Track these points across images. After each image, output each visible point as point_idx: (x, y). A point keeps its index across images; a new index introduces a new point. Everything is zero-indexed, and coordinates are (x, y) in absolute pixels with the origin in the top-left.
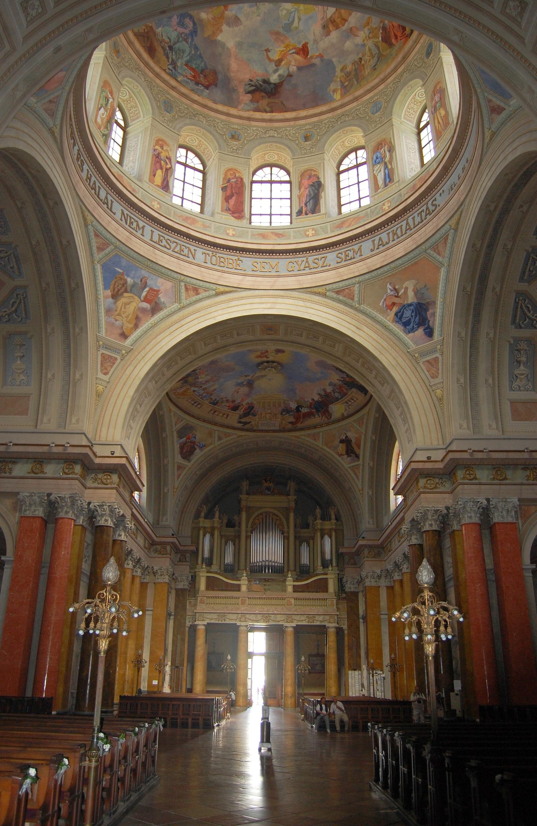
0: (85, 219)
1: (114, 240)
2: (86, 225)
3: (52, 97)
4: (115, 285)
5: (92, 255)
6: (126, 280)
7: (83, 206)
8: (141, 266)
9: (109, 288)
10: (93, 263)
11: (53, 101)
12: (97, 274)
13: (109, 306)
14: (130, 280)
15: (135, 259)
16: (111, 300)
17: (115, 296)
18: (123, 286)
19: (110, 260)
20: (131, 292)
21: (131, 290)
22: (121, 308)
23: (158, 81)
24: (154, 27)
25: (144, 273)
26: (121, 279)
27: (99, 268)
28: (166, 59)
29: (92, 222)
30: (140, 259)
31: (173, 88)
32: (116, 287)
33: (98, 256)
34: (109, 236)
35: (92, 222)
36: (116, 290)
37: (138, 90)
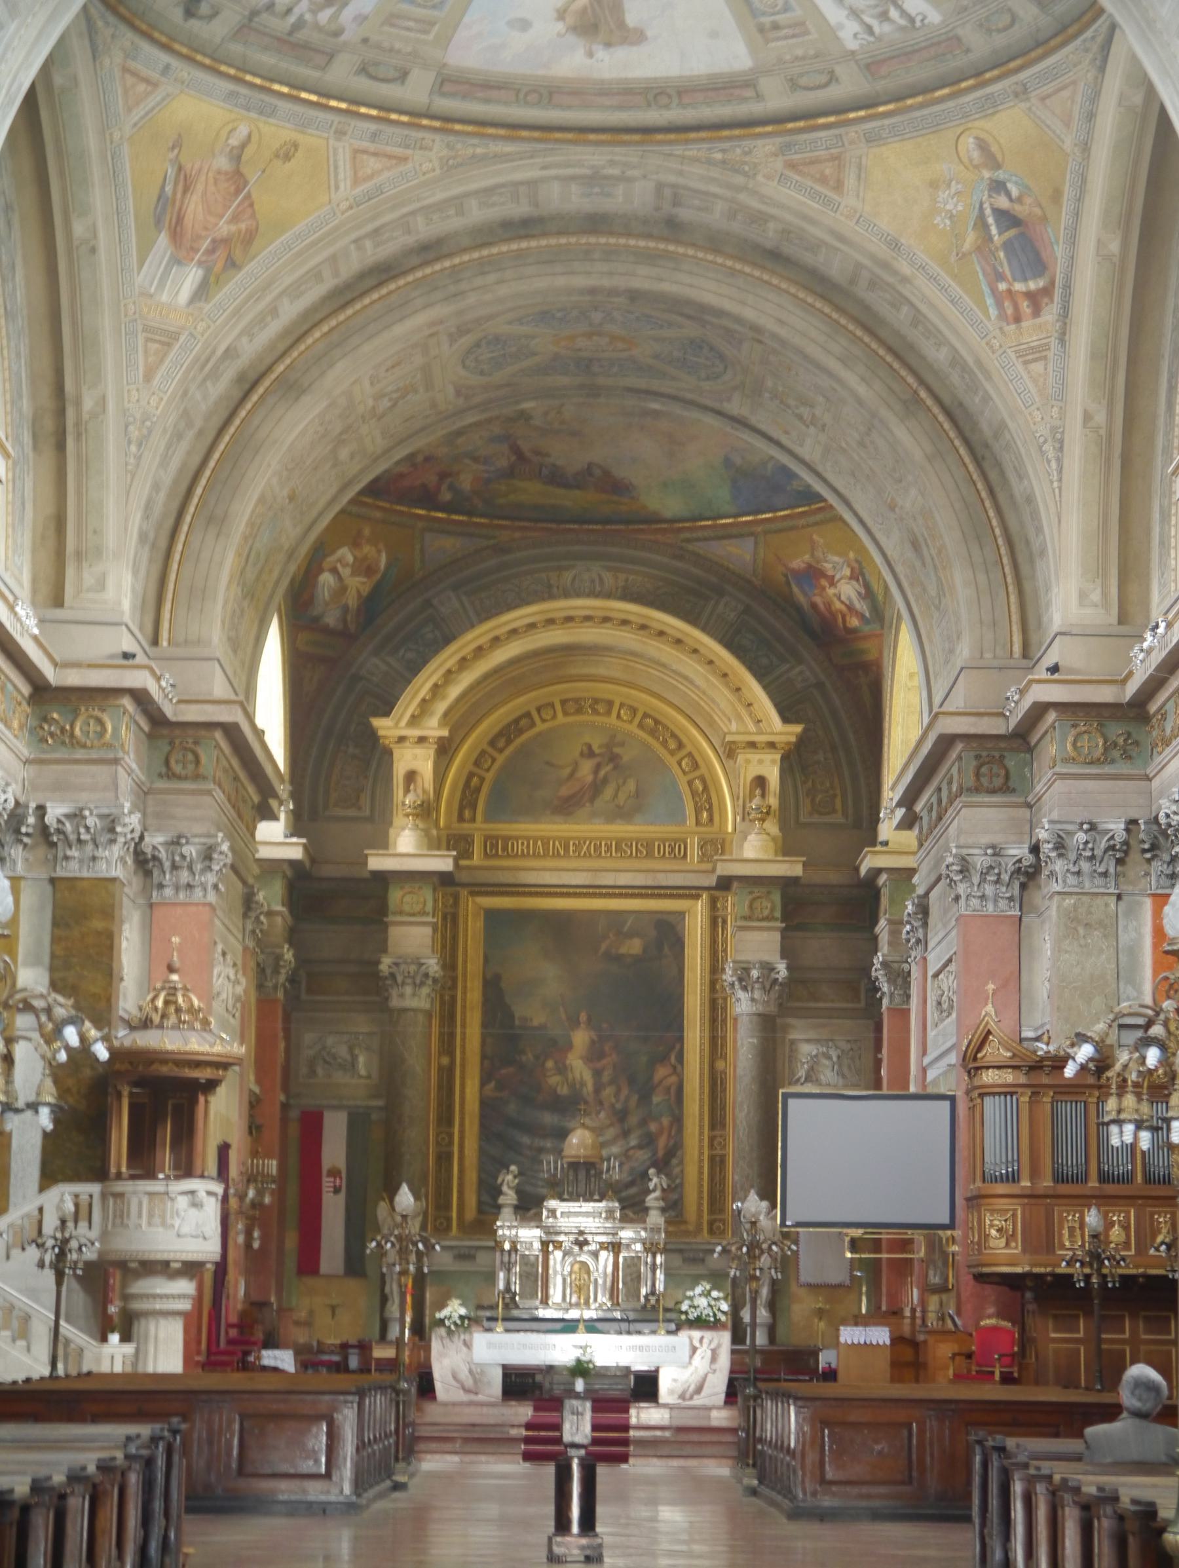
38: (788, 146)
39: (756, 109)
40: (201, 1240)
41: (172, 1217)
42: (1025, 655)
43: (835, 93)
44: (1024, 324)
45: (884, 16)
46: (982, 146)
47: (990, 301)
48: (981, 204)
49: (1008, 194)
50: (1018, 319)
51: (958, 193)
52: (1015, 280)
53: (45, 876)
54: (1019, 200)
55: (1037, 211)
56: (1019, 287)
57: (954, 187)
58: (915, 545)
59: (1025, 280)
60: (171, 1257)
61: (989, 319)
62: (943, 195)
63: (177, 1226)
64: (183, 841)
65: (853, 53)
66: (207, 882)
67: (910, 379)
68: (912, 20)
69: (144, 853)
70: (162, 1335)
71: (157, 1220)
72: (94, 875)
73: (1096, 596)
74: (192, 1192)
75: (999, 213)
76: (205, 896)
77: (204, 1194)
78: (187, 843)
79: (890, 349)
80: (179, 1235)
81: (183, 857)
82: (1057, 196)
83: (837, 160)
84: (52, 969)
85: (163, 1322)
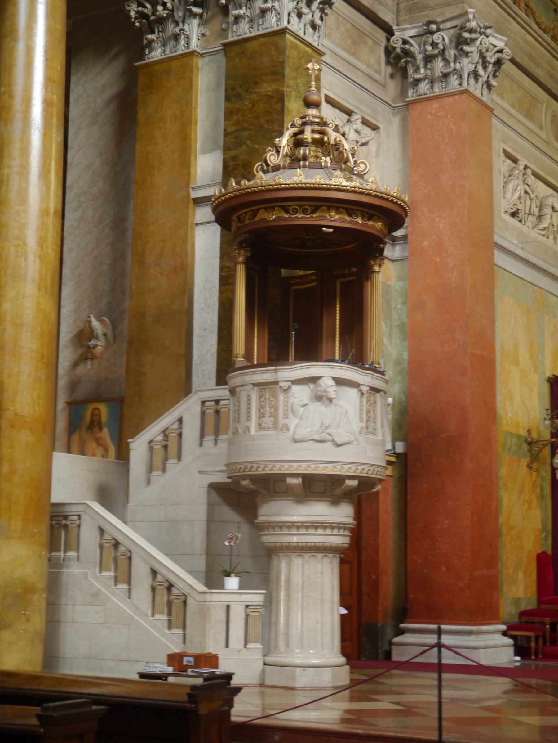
40: (329, 445)
41: (286, 416)
53: (217, 45)
60: (285, 469)
63: (292, 429)
64: (434, 27)
66: (462, 69)
69: (394, 48)
70: (297, 578)
71: (268, 420)
72: (262, 32)
74: (314, 380)
76: (460, 84)
77: (332, 383)
78: (439, 30)
80: (295, 441)
81: (434, 45)
84: (226, 149)
85: (297, 561)
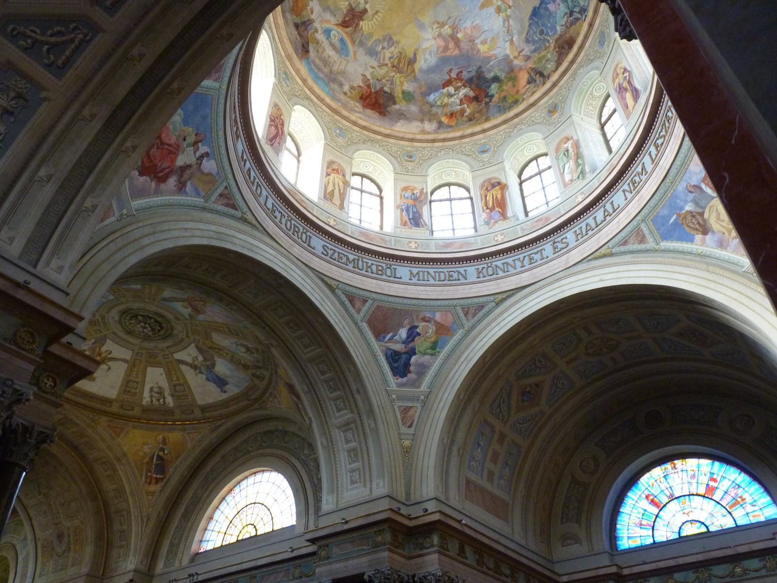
0: (605, 256)
1: (635, 223)
2: (611, 255)
3: (462, 315)
4: (690, 227)
5: (647, 251)
6: (687, 211)
7: (589, 258)
8: (672, 191)
9: (694, 235)
10: (657, 250)
11: (467, 311)
12: (672, 248)
13: (715, 241)
14: (689, 207)
15: (662, 197)
16: (709, 237)
17: (705, 230)
18: (694, 216)
19: (658, 229)
20: (704, 208)
21: (702, 207)
22: (723, 226)
23: (587, 45)
24: (556, 36)
25: (681, 187)
26: (685, 218)
27: (665, 245)
28: (579, 22)
29: (609, 248)
30: (661, 191)
31: (591, 25)
32: (693, 226)
33: (651, 244)
34: (629, 229)
35: (609, 248)
36: (697, 226)
37: (588, 80)
38: (111, 421)
39: (108, 409)
42: (102, 575)
43: (130, 413)
44: (151, 486)
45: (159, 400)
46: (164, 439)
47: (144, 477)
48: (154, 453)
49: (164, 452)
50: (150, 483)
51: (150, 448)
52: (154, 473)
54: (166, 455)
55: (170, 459)
56: (155, 476)
57: (150, 446)
58: (60, 537)
59: (157, 474)
61: (141, 480)
62: (145, 447)
65: (143, 405)
67: (97, 491)
68: (165, 403)
73: (144, 563)
75: (158, 455)
79: (95, 481)
82: (177, 458)
83: (122, 429)
